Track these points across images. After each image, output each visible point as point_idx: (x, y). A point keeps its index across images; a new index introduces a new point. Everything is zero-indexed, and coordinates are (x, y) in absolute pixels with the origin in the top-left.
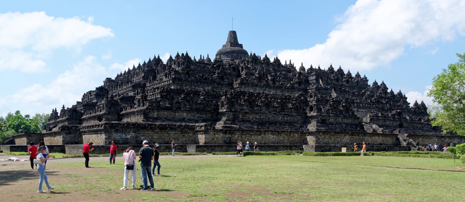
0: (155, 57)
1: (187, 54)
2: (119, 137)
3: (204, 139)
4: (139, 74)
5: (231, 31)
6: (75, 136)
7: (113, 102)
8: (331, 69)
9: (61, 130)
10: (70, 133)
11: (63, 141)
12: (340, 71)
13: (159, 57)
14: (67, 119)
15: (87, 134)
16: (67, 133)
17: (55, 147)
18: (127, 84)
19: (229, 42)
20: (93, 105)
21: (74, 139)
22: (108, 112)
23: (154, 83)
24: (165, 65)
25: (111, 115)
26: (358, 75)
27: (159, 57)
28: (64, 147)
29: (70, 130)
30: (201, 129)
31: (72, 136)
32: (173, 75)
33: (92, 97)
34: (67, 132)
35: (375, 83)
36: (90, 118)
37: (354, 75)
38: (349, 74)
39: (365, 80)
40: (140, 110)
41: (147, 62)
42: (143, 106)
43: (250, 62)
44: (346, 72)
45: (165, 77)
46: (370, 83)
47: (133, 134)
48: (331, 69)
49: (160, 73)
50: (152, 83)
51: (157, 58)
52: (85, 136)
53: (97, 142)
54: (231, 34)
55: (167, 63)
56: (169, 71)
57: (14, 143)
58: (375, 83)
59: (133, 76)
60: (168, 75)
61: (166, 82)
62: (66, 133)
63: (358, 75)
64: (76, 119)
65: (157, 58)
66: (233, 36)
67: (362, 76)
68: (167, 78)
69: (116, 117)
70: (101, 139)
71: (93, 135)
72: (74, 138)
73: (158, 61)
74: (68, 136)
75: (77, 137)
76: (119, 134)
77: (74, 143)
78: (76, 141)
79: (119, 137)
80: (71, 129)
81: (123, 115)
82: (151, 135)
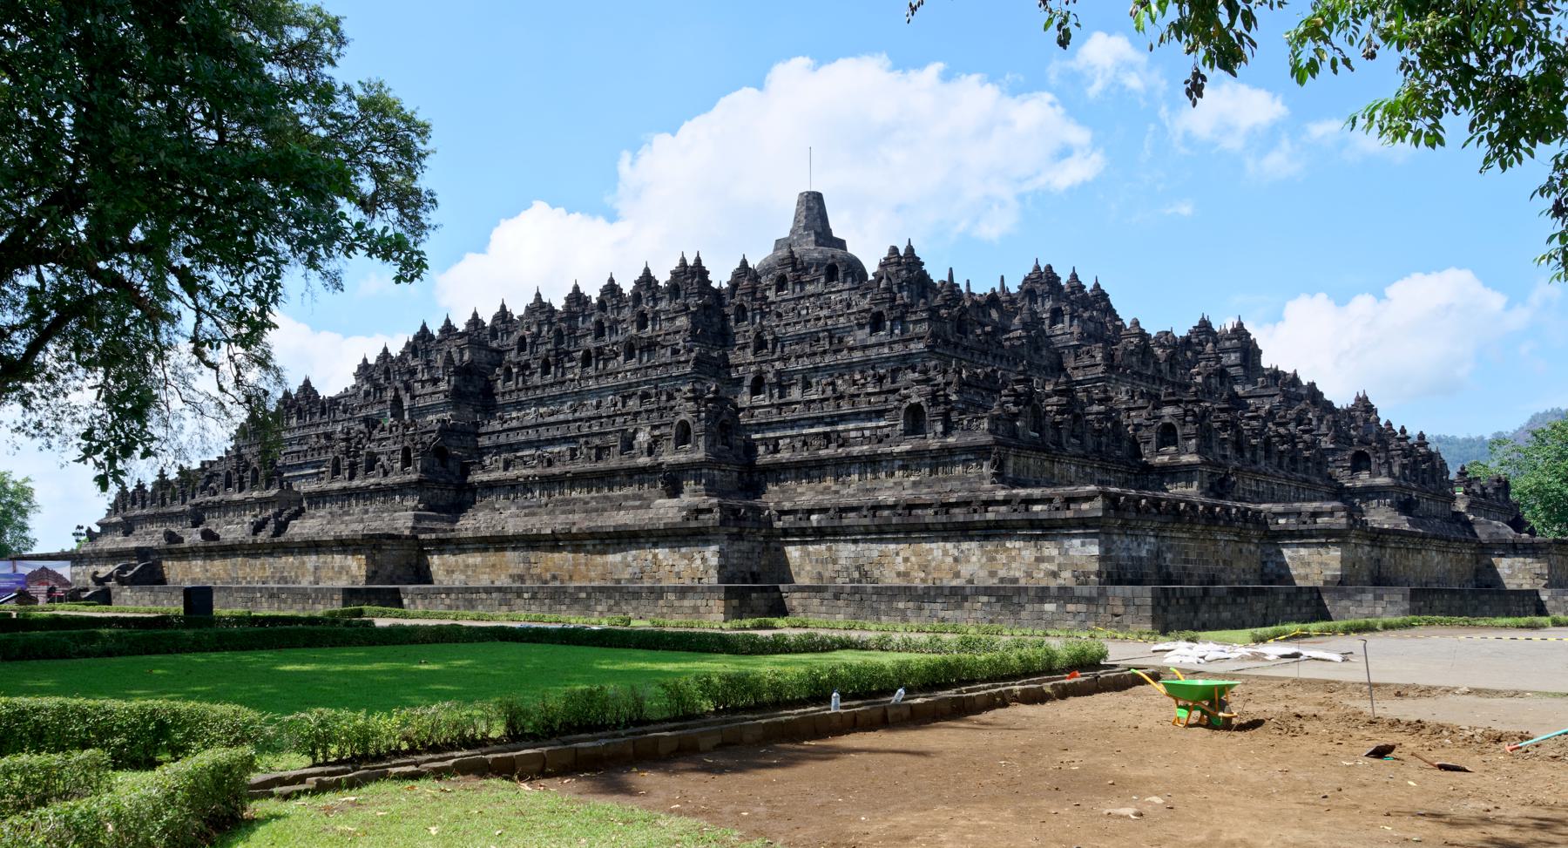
0: (683, 261)
1: (910, 249)
2: (1124, 554)
3: (1336, 564)
4: (653, 319)
5: (809, 193)
6: (753, 551)
7: (725, 417)
9: (723, 522)
10: (739, 537)
11: (721, 568)
13: (698, 260)
14: (419, 482)
15: (855, 542)
16: (733, 534)
17: (754, 595)
18: (641, 353)
19: (805, 228)
20: (469, 433)
21: (749, 563)
22: (714, 455)
23: (782, 351)
24: (718, 293)
25: (724, 466)
27: (698, 260)
28: (776, 595)
29: (743, 524)
30: (1314, 527)
31: (744, 546)
32: (916, 322)
33: (421, 403)
34: (735, 530)
36: (512, 488)
40: (942, 449)
41: (668, 277)
42: (946, 433)
43: (1041, 296)
45: (867, 330)
47: (1152, 540)
49: (753, 317)
50: (773, 352)
51: (690, 262)
52: (811, 548)
53: (983, 574)
54: (808, 201)
55: (734, 285)
56: (891, 308)
57: (158, 577)
59: (611, 328)
60: (892, 321)
61: (886, 350)
62: (730, 536)
64: (449, 483)
65: (690, 262)
66: (816, 211)
68: (528, 352)
69: (735, 475)
70: (1039, 560)
71: (926, 546)
72: (748, 558)
74: (735, 547)
75: (757, 550)
76: (1127, 541)
77: (748, 576)
78: (755, 568)
79: (1124, 554)
80: (745, 520)
81: (774, 470)
82: (1186, 547)
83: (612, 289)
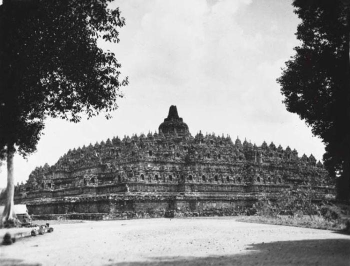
0: (114, 138)
8: (265, 144)
12: (272, 145)
13: (117, 137)
26: (288, 149)
27: (117, 137)
35: (305, 156)
37: (284, 148)
38: (280, 147)
39: (295, 153)
44: (277, 147)
46: (300, 155)
48: (265, 144)
58: (305, 156)
63: (288, 149)
65: (116, 137)
67: (292, 149)
73: (116, 141)
83: (102, 143)
